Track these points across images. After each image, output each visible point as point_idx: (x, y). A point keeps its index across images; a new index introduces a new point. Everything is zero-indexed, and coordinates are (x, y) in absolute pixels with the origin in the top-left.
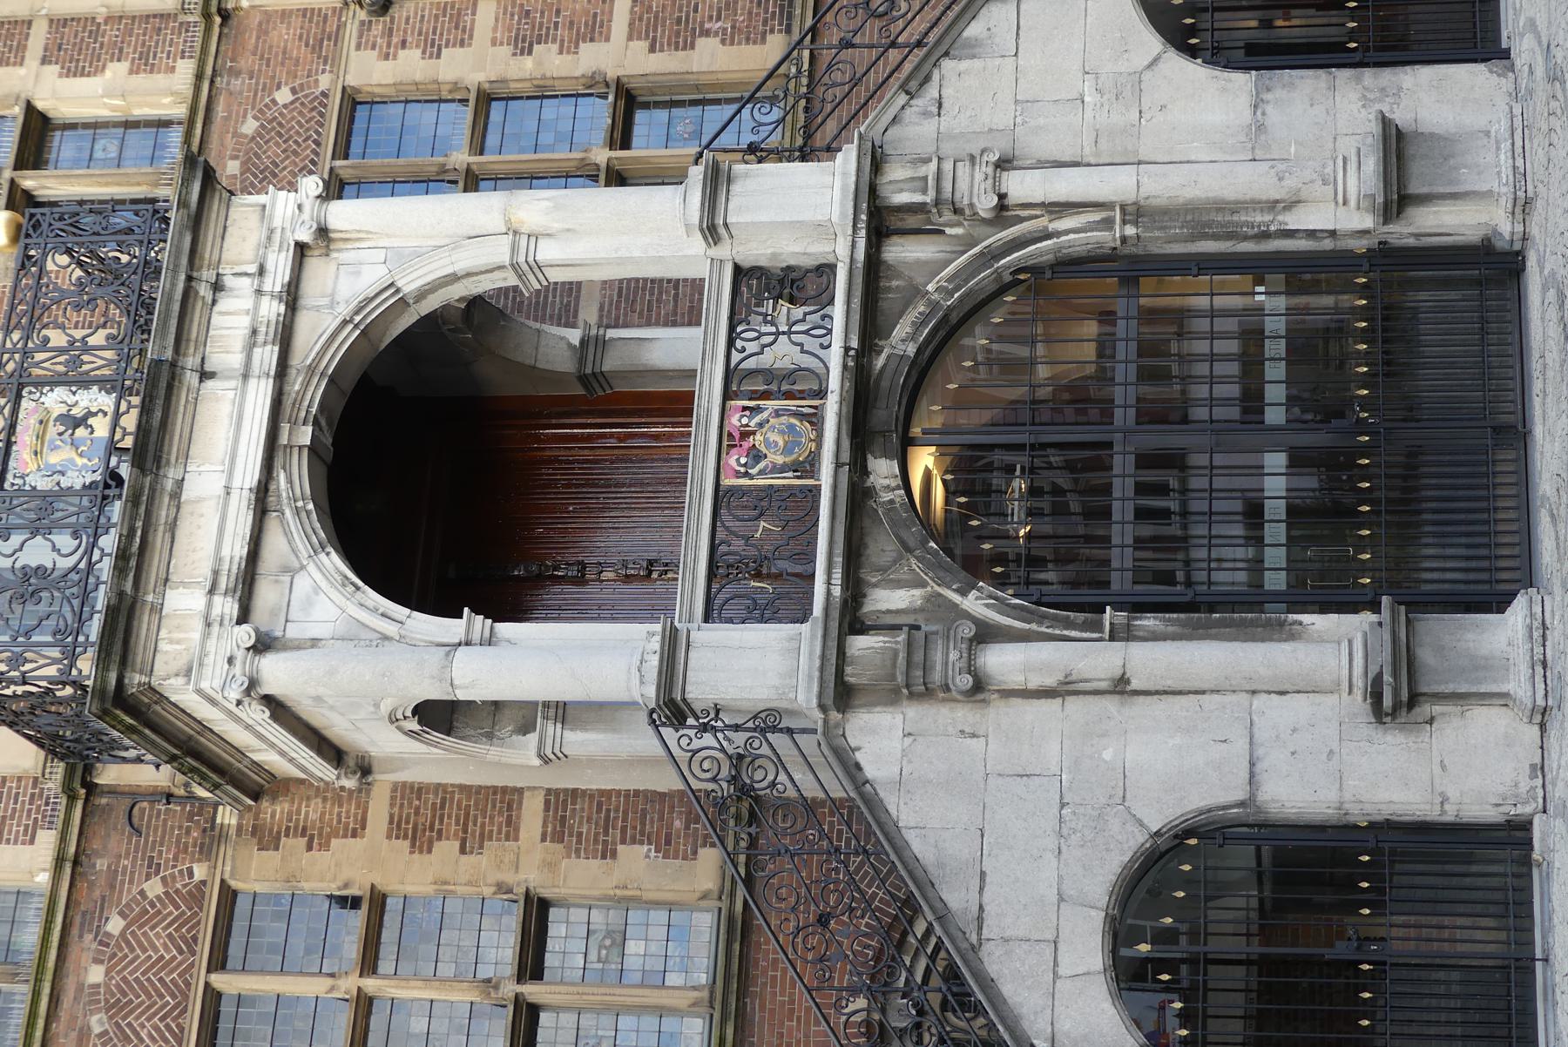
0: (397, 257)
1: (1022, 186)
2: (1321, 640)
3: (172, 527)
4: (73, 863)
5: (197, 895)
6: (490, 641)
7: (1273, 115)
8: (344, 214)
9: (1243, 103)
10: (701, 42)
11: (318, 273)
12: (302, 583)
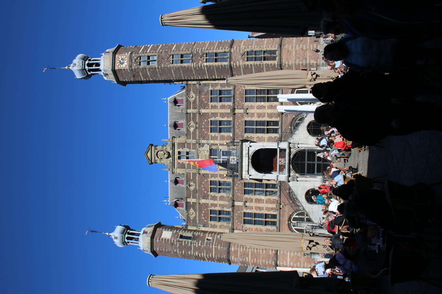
1: (299, 146)
4: (233, 181)
5: (242, 183)
8: (252, 144)
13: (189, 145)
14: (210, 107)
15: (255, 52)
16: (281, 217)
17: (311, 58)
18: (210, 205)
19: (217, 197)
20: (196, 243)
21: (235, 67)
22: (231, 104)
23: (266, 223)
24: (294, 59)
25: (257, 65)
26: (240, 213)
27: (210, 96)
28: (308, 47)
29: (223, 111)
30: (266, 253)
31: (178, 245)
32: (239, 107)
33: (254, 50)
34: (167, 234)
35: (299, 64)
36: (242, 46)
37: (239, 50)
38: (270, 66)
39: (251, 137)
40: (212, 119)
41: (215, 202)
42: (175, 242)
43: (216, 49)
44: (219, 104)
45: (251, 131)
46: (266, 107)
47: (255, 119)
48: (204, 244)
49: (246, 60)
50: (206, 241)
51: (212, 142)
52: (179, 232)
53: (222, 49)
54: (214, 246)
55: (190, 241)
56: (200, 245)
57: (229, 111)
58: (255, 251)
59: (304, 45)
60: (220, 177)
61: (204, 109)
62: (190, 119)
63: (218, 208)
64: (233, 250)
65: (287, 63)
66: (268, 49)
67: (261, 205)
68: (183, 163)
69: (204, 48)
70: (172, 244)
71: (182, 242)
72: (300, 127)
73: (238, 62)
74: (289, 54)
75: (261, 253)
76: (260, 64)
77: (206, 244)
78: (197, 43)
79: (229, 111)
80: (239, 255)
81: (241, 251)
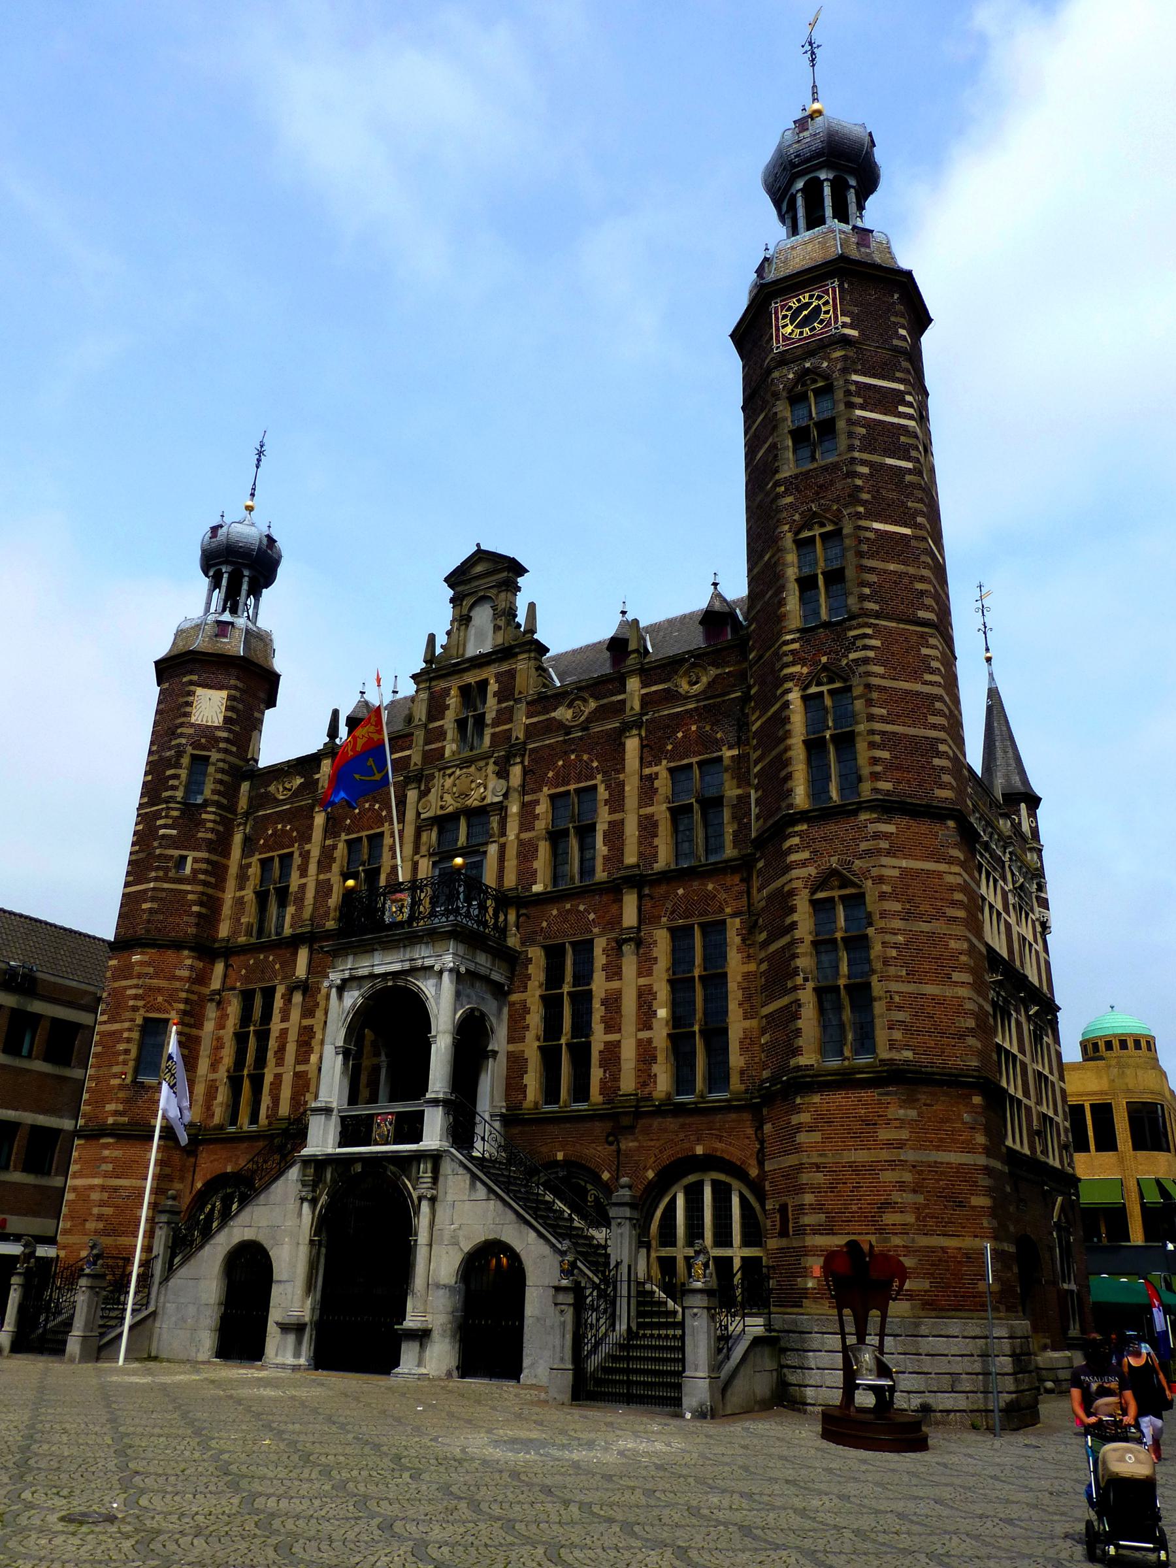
1: (425, 1207)
2: (303, 1303)
6: (337, 1054)
7: (441, 1292)
12: (356, 993)
13: (505, 716)
14: (647, 771)
15: (865, 937)
18: (307, 847)
19: (329, 869)
20: (167, 817)
23: (235, 1082)
24: (829, 1159)
25: (795, 956)
26: (274, 971)
27: (694, 760)
29: (631, 830)
30: (113, 1087)
31: (168, 754)
33: (870, 931)
34: (210, 706)
35: (800, 1189)
36: (892, 867)
37: (869, 853)
40: (601, 789)
41: (313, 868)
42: (178, 741)
43: (872, 732)
44: (660, 810)
45: (554, 977)
46: (644, 1035)
47: (599, 985)
48: (160, 846)
49: (820, 895)
51: (514, 809)
52: (219, 750)
53: (875, 761)
54: (152, 885)
55: (179, 794)
56: (161, 832)
57: (631, 859)
58: (121, 1047)
59: (910, 1218)
61: (642, 747)
63: (295, 881)
64: (135, 958)
65: (805, 1117)
66: (879, 1008)
67: (291, 1048)
68: (447, 707)
69: (879, 670)
70: (173, 733)
71: (178, 765)
73: (805, 855)
75: (116, 1069)
77: (160, 855)
78: (922, 636)
80: (116, 985)
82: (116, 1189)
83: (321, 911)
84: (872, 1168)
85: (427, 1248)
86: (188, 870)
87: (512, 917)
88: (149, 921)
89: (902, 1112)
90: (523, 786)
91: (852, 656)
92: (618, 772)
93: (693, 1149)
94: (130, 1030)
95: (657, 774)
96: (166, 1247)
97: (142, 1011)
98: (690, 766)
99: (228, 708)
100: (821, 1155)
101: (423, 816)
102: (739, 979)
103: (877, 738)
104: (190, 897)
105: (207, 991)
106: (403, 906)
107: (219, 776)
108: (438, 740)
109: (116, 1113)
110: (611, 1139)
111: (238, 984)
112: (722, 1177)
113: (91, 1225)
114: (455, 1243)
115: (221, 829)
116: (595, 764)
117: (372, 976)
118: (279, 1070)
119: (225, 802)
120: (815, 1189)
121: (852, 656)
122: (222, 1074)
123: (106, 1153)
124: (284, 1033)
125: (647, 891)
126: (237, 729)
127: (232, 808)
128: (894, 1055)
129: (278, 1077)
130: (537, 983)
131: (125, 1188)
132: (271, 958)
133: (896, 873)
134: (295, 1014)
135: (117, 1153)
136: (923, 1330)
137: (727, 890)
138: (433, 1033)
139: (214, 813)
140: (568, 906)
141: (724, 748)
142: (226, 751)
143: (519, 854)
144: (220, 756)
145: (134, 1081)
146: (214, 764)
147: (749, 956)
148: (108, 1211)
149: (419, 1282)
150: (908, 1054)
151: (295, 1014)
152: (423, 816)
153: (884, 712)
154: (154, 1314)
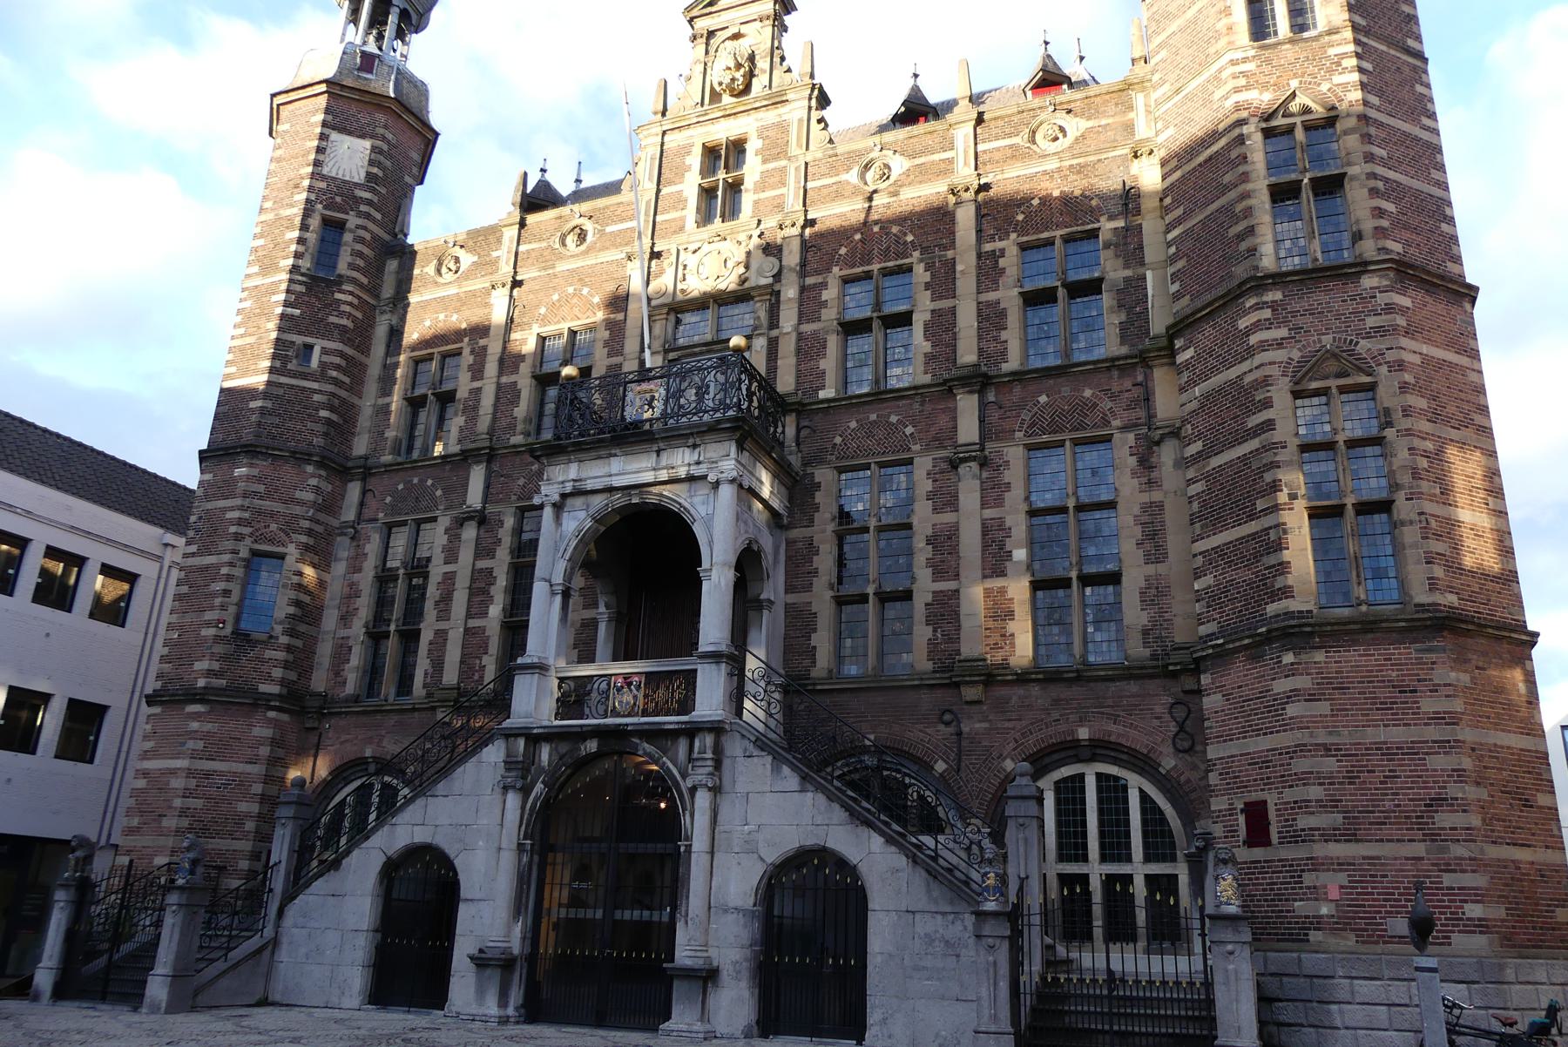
0: (709, 521)
1: (703, 800)
3: (599, 458)
6: (553, 594)
7: (731, 918)
8: (727, 492)
9: (739, 903)
10: (930, 628)
11: (702, 490)
12: (582, 514)
14: (988, 247)
16: (396, 718)
17: (1363, 874)
18: (482, 342)
21: (1243, 324)
22: (1012, 363)
24: (1345, 738)
25: (1275, 465)
27: (1058, 233)
28: (1459, 850)
32: (994, 415)
33: (1389, 433)
36: (1413, 350)
37: (1380, 331)
38: (1271, 560)
39: (817, 508)
40: (919, 269)
43: (1373, 176)
44: (1008, 296)
50: (299, 340)
51: (790, 292)
52: (360, 214)
53: (1379, 213)
57: (967, 355)
58: (219, 586)
59: (1475, 821)
60: (609, 367)
61: (980, 216)
62: (922, 153)
64: (237, 472)
65: (1302, 682)
67: (460, 599)
72: (821, 798)
73: (1283, 332)
74: (1384, 694)
75: (209, 616)
76: (1275, 487)
79: (967, 355)
80: (209, 506)
81: (230, 515)
82: (208, 775)
83: (504, 422)
84: (1413, 751)
85: (708, 857)
86: (314, 363)
87: (790, 431)
88: (259, 424)
89: (1453, 675)
90: (803, 264)
91: (1337, 79)
92: (946, 248)
93: (1073, 732)
94: (231, 564)
95: (1002, 251)
96: (291, 851)
97: (248, 541)
98: (1050, 243)
99: (371, 163)
100: (1330, 733)
101: (654, 303)
102: (1136, 510)
103: (1380, 185)
104: (316, 397)
105: (336, 523)
106: (653, 398)
107: (359, 247)
108: (675, 208)
109: (210, 673)
110: (947, 717)
111: (381, 515)
112: (1113, 770)
113: (170, 823)
114: (751, 849)
115: (359, 315)
116: (910, 238)
117: (610, 490)
118: (442, 625)
119: (365, 281)
120: (1322, 779)
121: (1337, 79)
122: (358, 629)
123: (195, 725)
124: (449, 578)
125: (991, 397)
126: (383, 191)
127: (374, 290)
128: (1438, 598)
129: (441, 635)
130: (828, 516)
131: (221, 774)
132: (429, 482)
133: (1417, 359)
134: (466, 555)
135: (208, 727)
136: (1510, 974)
137: (1113, 397)
138: (705, 564)
139: (351, 293)
140: (873, 417)
141: (1103, 219)
142: (368, 216)
143: (798, 351)
144: (360, 221)
145: (236, 632)
146: (351, 231)
147: (1150, 482)
148: (197, 803)
149: (695, 901)
150: (1452, 599)
151: (466, 555)
152: (654, 303)
153: (1383, 153)
154: (275, 942)
